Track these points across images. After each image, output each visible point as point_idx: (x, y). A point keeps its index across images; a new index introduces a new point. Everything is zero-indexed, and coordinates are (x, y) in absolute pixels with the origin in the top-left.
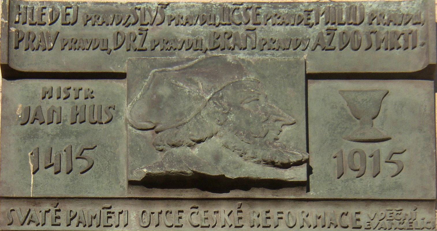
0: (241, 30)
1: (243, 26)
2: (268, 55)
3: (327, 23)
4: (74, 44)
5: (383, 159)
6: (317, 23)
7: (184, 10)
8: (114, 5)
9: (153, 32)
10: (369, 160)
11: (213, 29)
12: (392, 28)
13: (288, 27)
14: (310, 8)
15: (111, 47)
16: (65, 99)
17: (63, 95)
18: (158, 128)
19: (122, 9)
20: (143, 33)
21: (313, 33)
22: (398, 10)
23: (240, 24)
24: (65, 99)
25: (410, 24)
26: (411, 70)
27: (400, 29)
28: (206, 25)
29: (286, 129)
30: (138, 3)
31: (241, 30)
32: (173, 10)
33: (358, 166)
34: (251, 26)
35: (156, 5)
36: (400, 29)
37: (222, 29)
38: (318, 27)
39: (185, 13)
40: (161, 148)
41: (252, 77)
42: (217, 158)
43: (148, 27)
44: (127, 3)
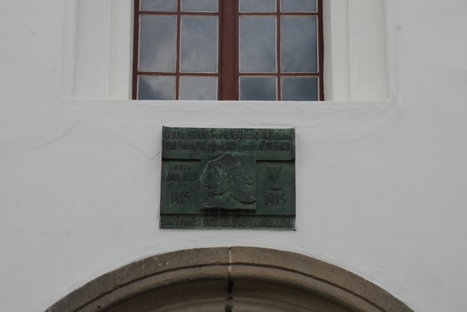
1: (237, 139)
2: (244, 153)
3: (262, 139)
4: (185, 147)
5: (280, 197)
6: (260, 139)
8: (197, 129)
9: (210, 141)
10: (275, 197)
11: (228, 140)
13: (251, 140)
14: (257, 132)
16: (181, 169)
17: (181, 168)
18: (210, 186)
22: (284, 133)
23: (236, 138)
24: (181, 169)
25: (288, 139)
26: (288, 159)
27: (284, 141)
28: (225, 138)
29: (250, 186)
31: (236, 141)
32: (215, 132)
34: (239, 139)
36: (284, 141)
37: (231, 140)
38: (260, 140)
40: (211, 195)
41: (239, 164)
42: (228, 201)
43: (207, 139)
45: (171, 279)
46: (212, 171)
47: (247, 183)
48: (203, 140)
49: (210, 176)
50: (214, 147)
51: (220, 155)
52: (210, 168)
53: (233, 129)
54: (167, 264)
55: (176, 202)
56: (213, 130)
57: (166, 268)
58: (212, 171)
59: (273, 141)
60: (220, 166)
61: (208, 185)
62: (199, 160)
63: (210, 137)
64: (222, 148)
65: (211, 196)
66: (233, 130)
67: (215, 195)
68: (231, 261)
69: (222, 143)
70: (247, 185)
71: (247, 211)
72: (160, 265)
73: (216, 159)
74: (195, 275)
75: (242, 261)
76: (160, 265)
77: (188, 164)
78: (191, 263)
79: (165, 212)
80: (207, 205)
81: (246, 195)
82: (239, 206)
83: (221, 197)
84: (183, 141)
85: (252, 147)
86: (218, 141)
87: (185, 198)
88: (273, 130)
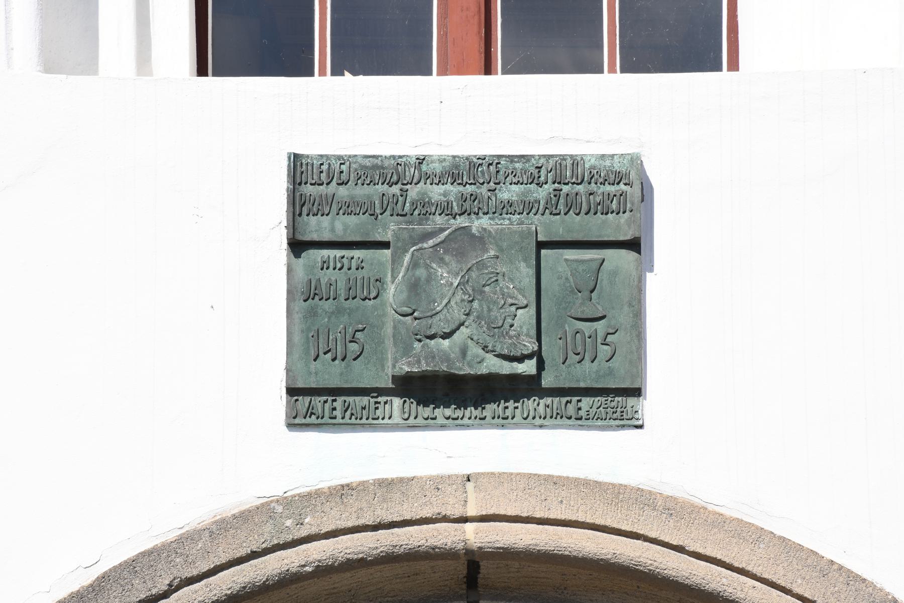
0: (484, 190)
2: (505, 223)
3: (554, 183)
5: (599, 341)
6: (546, 183)
7: (437, 165)
9: (414, 192)
11: (461, 188)
12: (608, 188)
15: (378, 211)
19: (386, 163)
20: (404, 192)
21: (542, 193)
23: (483, 183)
27: (611, 189)
30: (400, 157)
33: (580, 349)
35: (414, 159)
36: (611, 189)
38: (545, 186)
39: (437, 168)
40: (418, 337)
44: (391, 157)
45: (319, 561)
46: (421, 272)
47: (512, 305)
48: (396, 189)
49: (414, 287)
50: (424, 208)
51: (442, 230)
52: (414, 264)
53: (475, 156)
54: (307, 520)
55: (329, 356)
56: (421, 160)
57: (304, 532)
58: (421, 272)
59: (580, 188)
60: (441, 261)
61: (409, 311)
62: (385, 245)
63: (415, 181)
64: (446, 209)
65: (420, 341)
66: (475, 160)
67: (432, 337)
68: (471, 512)
69: (445, 194)
70: (513, 308)
71: (514, 378)
72: (289, 523)
73: (431, 243)
74: (381, 549)
75: (502, 512)
76: (289, 523)
77: (357, 253)
78: (368, 519)
79: (300, 385)
80: (409, 364)
81: (511, 337)
82: (493, 365)
83: (446, 343)
84: (343, 191)
85: (528, 207)
86: (436, 192)
87: (354, 347)
88: (582, 159)
